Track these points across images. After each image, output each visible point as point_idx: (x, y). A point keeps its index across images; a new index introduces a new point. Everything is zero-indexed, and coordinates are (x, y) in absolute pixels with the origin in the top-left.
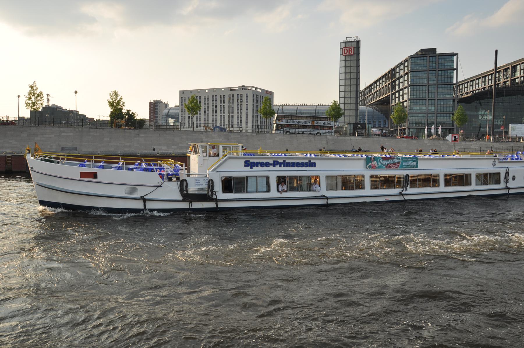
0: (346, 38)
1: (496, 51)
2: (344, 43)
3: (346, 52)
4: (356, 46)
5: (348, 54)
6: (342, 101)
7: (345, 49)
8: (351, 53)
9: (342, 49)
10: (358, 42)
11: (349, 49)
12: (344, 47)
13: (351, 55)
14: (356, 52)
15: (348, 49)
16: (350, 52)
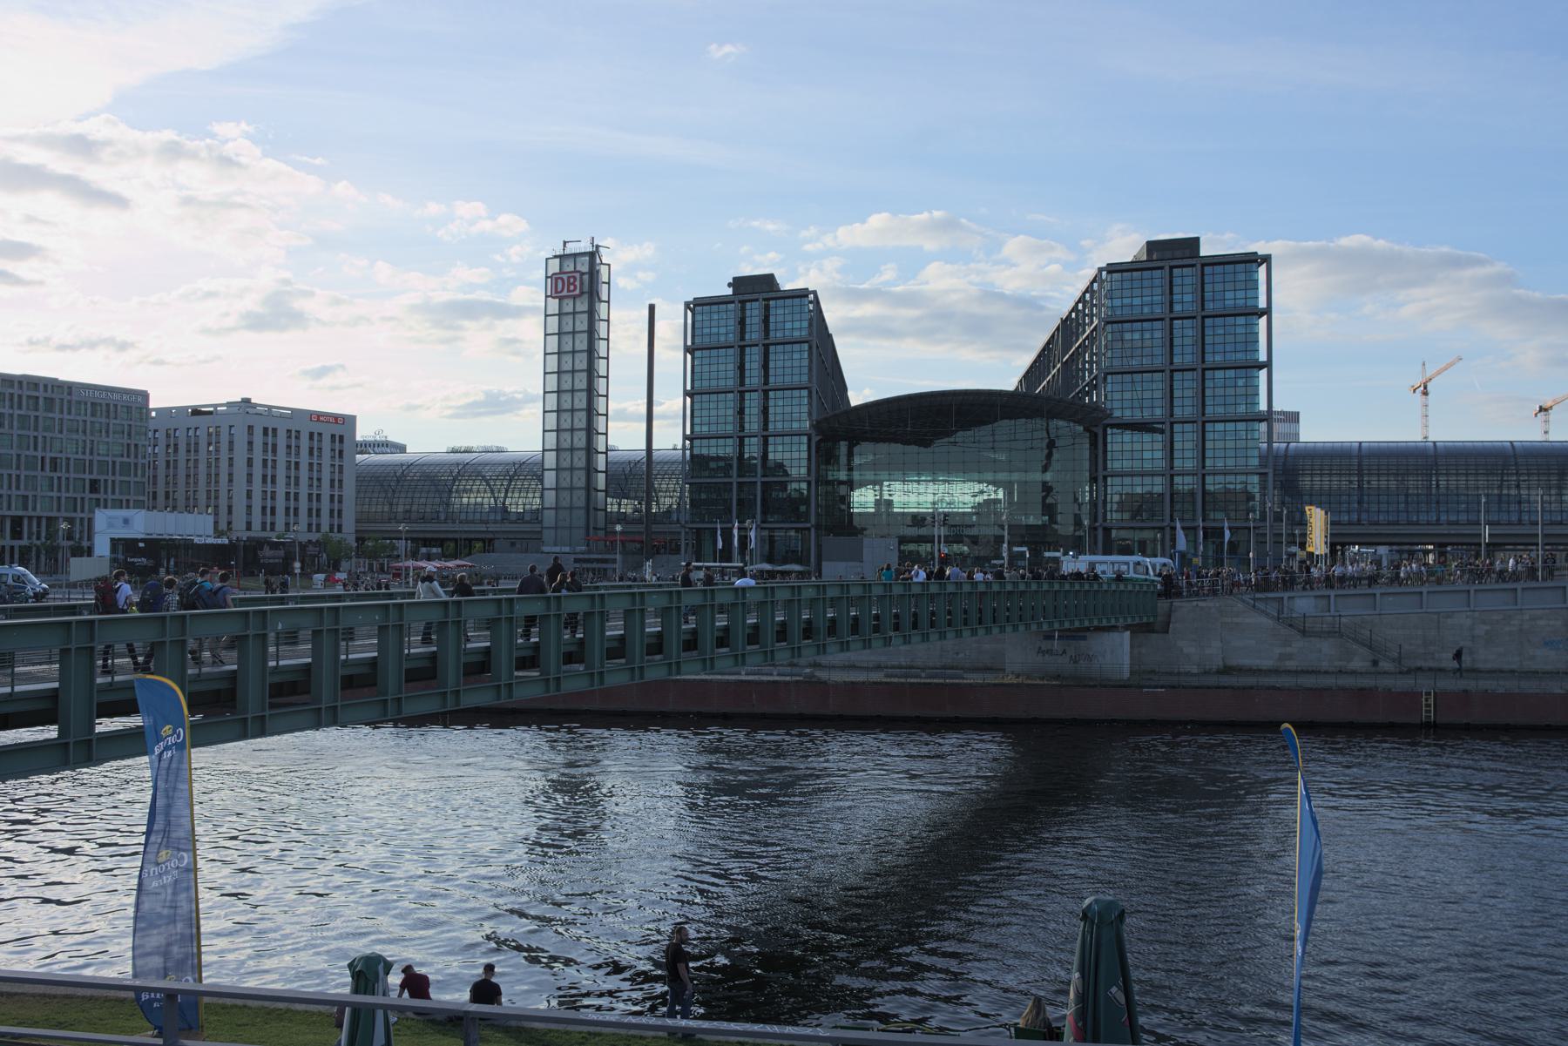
0: (565, 243)
1: (652, 308)
2: (558, 260)
3: (559, 289)
4: (585, 269)
5: (565, 293)
6: (552, 438)
7: (557, 279)
8: (574, 290)
9: (551, 277)
10: (593, 255)
11: (569, 278)
12: (558, 271)
13: (574, 297)
14: (586, 288)
15: (565, 277)
16: (572, 288)
